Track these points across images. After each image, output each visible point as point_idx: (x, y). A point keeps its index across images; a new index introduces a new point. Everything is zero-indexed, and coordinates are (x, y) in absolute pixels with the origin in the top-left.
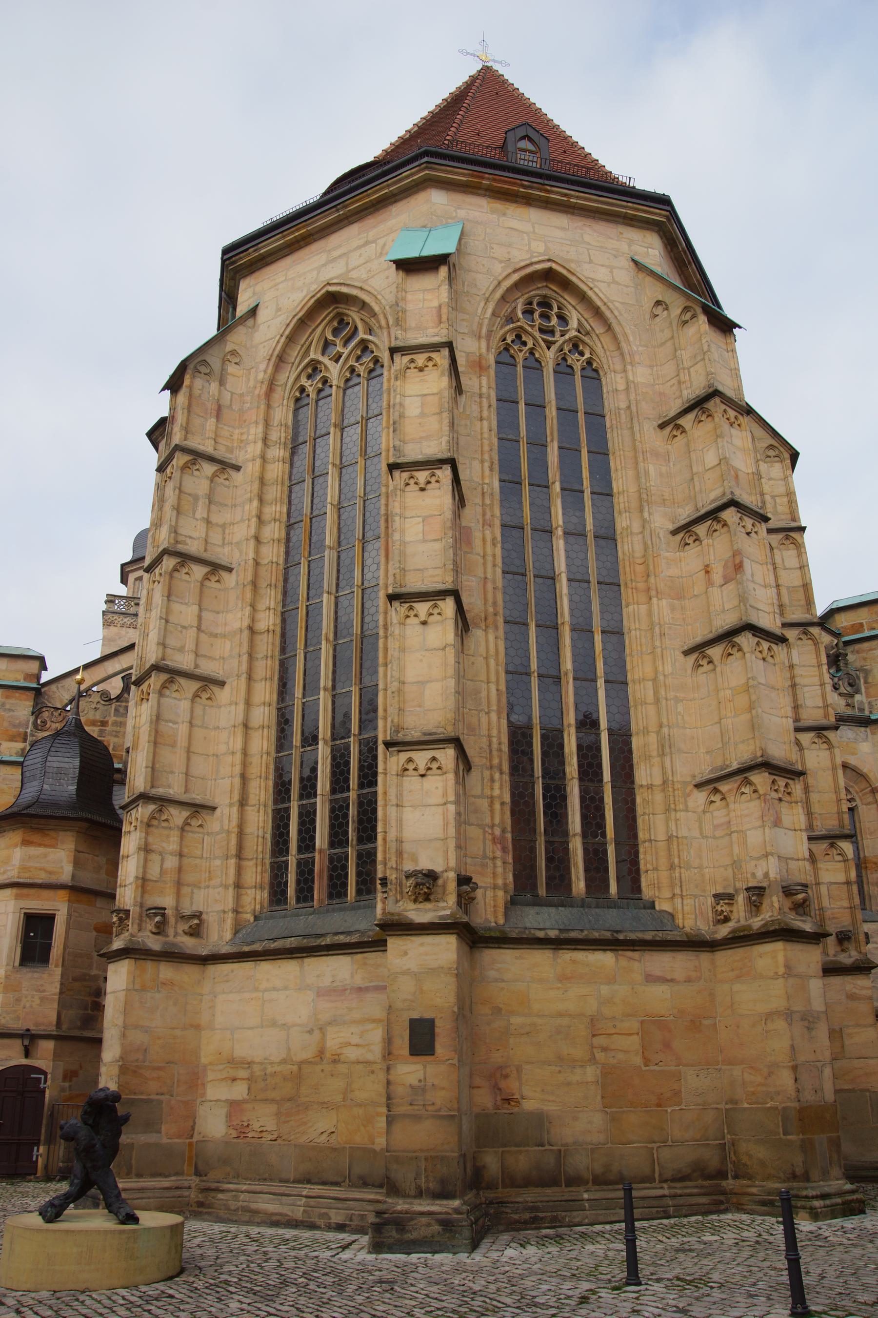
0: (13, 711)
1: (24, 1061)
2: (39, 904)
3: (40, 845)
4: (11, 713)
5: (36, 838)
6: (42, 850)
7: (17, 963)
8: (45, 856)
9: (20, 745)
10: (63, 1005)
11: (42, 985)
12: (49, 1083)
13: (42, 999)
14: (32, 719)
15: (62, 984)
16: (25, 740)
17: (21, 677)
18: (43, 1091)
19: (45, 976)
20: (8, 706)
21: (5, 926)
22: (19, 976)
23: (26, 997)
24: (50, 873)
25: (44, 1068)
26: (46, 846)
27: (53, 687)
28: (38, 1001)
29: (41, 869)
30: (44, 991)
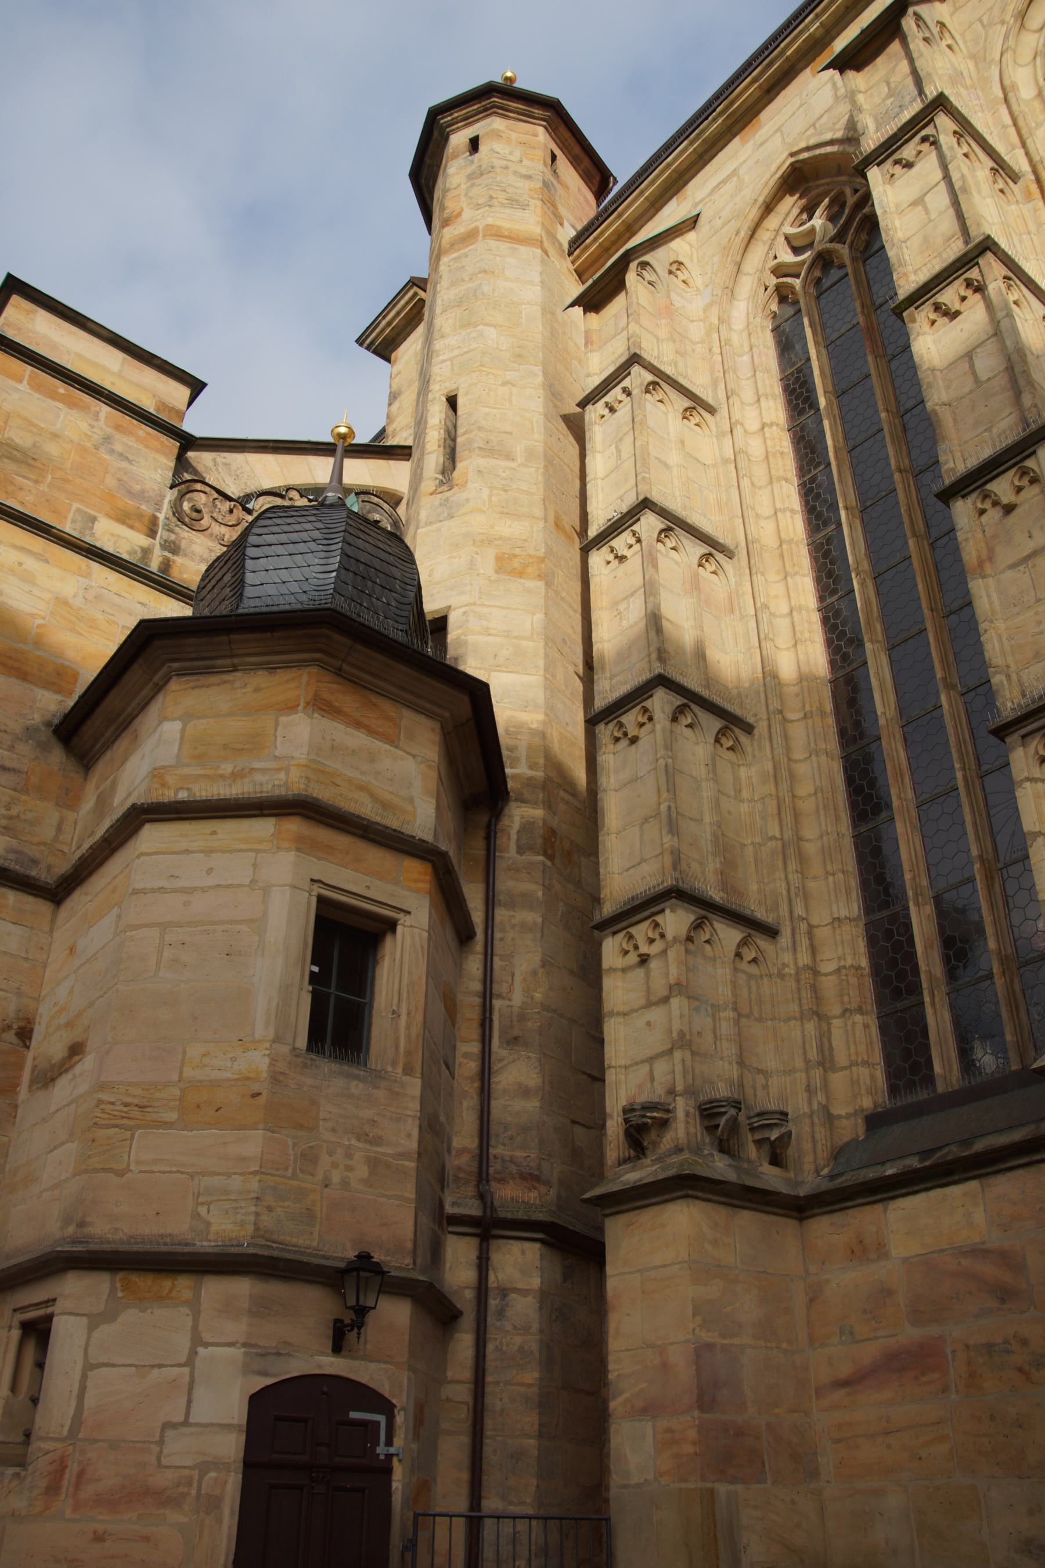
0: (130, 462)
1: (331, 1364)
3: (358, 725)
4: (125, 464)
5: (348, 700)
6: (358, 739)
7: (302, 1042)
8: (372, 758)
11: (373, 1123)
12: (399, 1441)
13: (374, 1164)
14: (170, 495)
16: (152, 533)
19: (381, 1094)
22: (310, 1081)
23: (330, 1153)
24: (385, 805)
25: (386, 1390)
26: (371, 732)
28: (362, 1171)
29: (362, 788)
30: (377, 1141)
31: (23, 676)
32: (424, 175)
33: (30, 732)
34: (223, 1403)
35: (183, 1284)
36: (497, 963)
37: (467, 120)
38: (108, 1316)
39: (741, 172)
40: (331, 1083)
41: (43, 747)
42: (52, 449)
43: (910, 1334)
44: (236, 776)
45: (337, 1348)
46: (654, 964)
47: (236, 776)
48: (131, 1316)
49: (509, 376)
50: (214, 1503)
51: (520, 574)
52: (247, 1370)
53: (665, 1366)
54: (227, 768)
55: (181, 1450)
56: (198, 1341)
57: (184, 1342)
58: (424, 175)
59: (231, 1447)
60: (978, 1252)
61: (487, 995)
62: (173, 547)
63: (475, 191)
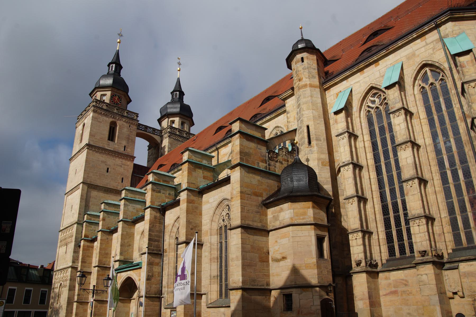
1: (327, 297)
2: (320, 233)
9: (265, 165)
13: (328, 271)
17: (260, 136)
21: (311, 241)
31: (257, 196)
32: (289, 61)
34: (317, 302)
37: (301, 53)
38: (302, 294)
39: (361, 82)
41: (262, 207)
42: (251, 151)
43: (393, 289)
44: (303, 219)
46: (357, 240)
47: (303, 219)
48: (304, 293)
49: (318, 122)
51: (325, 166)
53: (364, 294)
54: (301, 217)
55: (313, 308)
56: (313, 296)
57: (312, 296)
58: (289, 61)
59: (319, 307)
60: (403, 280)
62: (269, 165)
63: (305, 73)
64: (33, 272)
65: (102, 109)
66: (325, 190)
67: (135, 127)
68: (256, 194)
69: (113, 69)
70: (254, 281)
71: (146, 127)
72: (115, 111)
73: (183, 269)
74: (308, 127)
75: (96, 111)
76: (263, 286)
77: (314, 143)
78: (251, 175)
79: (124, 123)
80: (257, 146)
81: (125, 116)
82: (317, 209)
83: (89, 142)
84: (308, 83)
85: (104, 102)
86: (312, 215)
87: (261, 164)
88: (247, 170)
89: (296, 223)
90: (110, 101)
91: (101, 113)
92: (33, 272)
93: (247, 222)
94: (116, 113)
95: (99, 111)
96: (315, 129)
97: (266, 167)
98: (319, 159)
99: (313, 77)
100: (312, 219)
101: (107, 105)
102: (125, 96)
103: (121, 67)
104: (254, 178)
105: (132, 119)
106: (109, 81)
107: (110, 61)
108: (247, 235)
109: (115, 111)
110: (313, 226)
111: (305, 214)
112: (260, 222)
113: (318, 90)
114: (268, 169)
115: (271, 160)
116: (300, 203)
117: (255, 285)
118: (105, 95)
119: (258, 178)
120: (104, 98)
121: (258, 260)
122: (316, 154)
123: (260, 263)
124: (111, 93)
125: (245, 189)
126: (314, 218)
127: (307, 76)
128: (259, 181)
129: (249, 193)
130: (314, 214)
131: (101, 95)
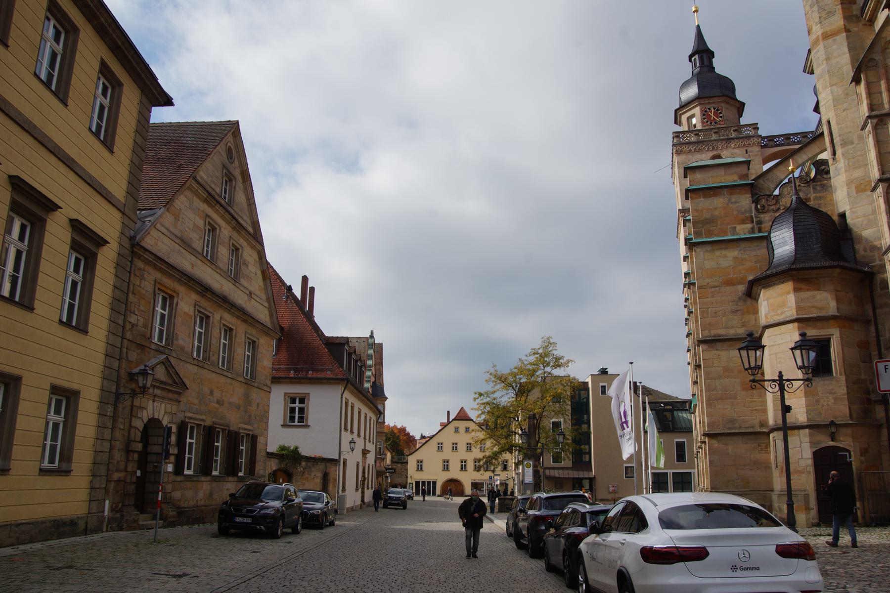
6: (809, 294)
8: (814, 297)
9: (749, 226)
10: (851, 402)
12: (853, 458)
13: (835, 399)
14: (753, 206)
15: (847, 387)
16: (752, 222)
17: (735, 177)
18: (850, 464)
20: (733, 200)
24: (821, 309)
25: (847, 447)
27: (761, 181)
30: (835, 393)
31: (733, 284)
33: (740, 298)
35: (796, 431)
36: (879, 326)
40: (820, 384)
41: (745, 301)
42: (717, 213)
44: (782, 313)
45: (833, 440)
49: (845, 105)
50: (809, 473)
52: (811, 447)
54: (779, 312)
56: (801, 443)
59: (810, 462)
61: (878, 336)
64: (684, 415)
65: (689, 143)
66: (867, 240)
67: (756, 149)
68: (730, 283)
69: (698, 65)
70: (732, 421)
71: (787, 137)
72: (714, 137)
73: (625, 412)
74: (829, 122)
75: (681, 151)
76: (753, 427)
77: (839, 152)
78: (718, 253)
79: (735, 150)
80: (730, 200)
81: (733, 139)
82: (808, 290)
83: (683, 206)
84: (820, 33)
85: (692, 130)
86: (794, 305)
87: (739, 228)
88: (708, 248)
89: (772, 322)
90: (703, 122)
91: (690, 150)
92: (684, 415)
93: (713, 332)
94: (715, 140)
95: (686, 149)
96: (838, 124)
97: (753, 229)
98: (849, 183)
99: (830, 14)
100: (795, 313)
101: (697, 133)
102: (727, 103)
103: (711, 54)
104: (725, 256)
105: (749, 137)
106: (693, 91)
107: (690, 52)
108: (714, 352)
109: (714, 137)
110: (796, 324)
111: (783, 304)
112: (743, 326)
113: (842, 38)
114: (756, 231)
115: (763, 213)
116: (776, 287)
117: (735, 428)
118: (693, 116)
119: (733, 253)
120: (694, 121)
121: (739, 388)
122: (844, 175)
123: (744, 393)
124: (702, 111)
125: (708, 280)
126: (799, 309)
127: (817, 20)
128: (735, 258)
129: (715, 284)
130: (796, 302)
131: (688, 118)
